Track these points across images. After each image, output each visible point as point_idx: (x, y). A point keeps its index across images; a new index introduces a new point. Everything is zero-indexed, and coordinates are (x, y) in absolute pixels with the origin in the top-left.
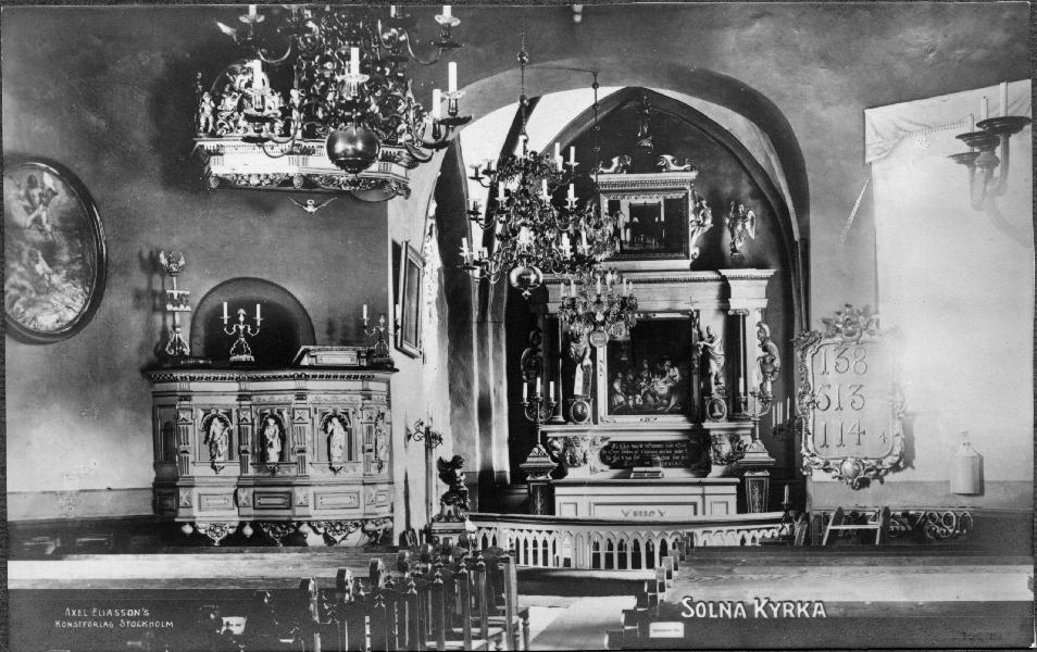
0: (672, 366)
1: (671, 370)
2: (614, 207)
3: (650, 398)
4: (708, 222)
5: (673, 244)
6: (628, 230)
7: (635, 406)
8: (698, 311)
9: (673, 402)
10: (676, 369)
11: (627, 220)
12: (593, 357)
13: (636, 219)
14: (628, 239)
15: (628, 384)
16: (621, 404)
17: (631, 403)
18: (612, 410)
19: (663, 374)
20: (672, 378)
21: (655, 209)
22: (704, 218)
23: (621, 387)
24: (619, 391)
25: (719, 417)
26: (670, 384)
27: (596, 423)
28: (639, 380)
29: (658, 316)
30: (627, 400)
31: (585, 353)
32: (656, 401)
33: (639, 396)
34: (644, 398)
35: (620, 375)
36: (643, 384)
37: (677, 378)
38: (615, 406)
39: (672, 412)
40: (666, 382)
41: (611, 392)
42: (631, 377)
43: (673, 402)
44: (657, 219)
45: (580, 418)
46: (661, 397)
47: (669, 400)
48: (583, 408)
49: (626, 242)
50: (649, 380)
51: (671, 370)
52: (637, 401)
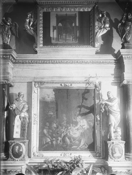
1: (81, 121)
2: (47, 17)
4: (107, 25)
5: (85, 37)
6: (55, 31)
7: (57, 145)
8: (100, 84)
9: (82, 143)
11: (55, 25)
12: (29, 111)
13: (60, 24)
14: (55, 36)
18: (44, 147)
21: (73, 18)
22: (105, 23)
23: (48, 132)
25: (119, 158)
26: (81, 131)
27: (30, 157)
28: (60, 127)
31: (23, 108)
32: (71, 142)
33: (60, 138)
35: (48, 124)
39: (82, 150)
40: (78, 129)
41: (42, 136)
42: (55, 125)
43: (82, 143)
44: (73, 25)
45: (18, 155)
48: (19, 148)
49: (53, 38)
51: (81, 121)
52: (59, 142)
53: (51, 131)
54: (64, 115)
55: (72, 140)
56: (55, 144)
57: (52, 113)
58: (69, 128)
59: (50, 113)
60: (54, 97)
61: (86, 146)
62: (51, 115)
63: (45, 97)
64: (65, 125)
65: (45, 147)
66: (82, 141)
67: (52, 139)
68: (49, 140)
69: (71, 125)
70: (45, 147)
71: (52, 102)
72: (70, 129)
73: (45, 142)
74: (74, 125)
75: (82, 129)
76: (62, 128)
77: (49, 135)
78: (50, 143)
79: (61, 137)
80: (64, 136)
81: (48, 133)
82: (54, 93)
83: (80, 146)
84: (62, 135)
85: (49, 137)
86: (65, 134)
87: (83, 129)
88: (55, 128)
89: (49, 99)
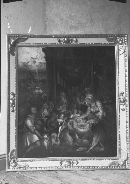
0: (94, 100)
3: (69, 138)
9: (94, 143)
10: (99, 104)
15: (42, 121)
16: (33, 144)
17: (46, 143)
19: (83, 109)
20: (94, 114)
23: (35, 124)
24: (33, 129)
26: (92, 121)
29: (81, 41)
30: (41, 140)
32: (74, 140)
33: (55, 135)
34: (63, 139)
35: (33, 109)
36: (60, 120)
37: (100, 114)
38: (28, 147)
43: (94, 143)
46: (81, 135)
47: (91, 142)
50: (67, 116)
51: (93, 105)
53: (39, 122)
54: (63, 94)
55: (77, 136)
56: (47, 146)
57: (41, 91)
58: (72, 116)
59: (37, 91)
60: (43, 61)
61: (102, 147)
62: (40, 95)
63: (28, 62)
64: (64, 110)
65: (29, 150)
66: (94, 139)
67: (42, 137)
68: (36, 138)
69: (76, 111)
70: (29, 150)
71: (41, 72)
72: (73, 118)
73: (30, 141)
74: (80, 112)
75: (94, 118)
76: (59, 118)
77: (37, 129)
78: (38, 143)
79: (57, 133)
80: (63, 131)
81: (35, 126)
82: (43, 54)
83: (91, 148)
84: (60, 129)
85: (37, 132)
86: (64, 127)
87: (95, 118)
88: (46, 117)
89: (34, 67)
